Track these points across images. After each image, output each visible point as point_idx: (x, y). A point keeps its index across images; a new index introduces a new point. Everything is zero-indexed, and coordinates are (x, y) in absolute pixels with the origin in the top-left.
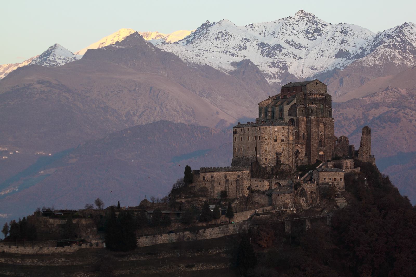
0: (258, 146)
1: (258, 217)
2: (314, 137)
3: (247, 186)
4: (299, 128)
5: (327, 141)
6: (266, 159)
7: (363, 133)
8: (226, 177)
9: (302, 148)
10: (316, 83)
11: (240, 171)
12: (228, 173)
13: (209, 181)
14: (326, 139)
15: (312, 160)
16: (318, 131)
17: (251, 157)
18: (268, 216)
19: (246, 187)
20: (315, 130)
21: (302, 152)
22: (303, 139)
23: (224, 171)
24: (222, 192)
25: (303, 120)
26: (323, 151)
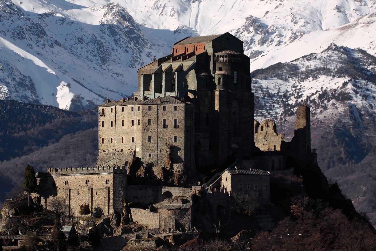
1: (138, 244)
4: (201, 108)
6: (150, 156)
7: (299, 115)
8: (87, 182)
10: (226, 38)
11: (110, 173)
12: (91, 176)
13: (62, 189)
17: (127, 152)
18: (153, 243)
23: (85, 174)
24: (82, 206)
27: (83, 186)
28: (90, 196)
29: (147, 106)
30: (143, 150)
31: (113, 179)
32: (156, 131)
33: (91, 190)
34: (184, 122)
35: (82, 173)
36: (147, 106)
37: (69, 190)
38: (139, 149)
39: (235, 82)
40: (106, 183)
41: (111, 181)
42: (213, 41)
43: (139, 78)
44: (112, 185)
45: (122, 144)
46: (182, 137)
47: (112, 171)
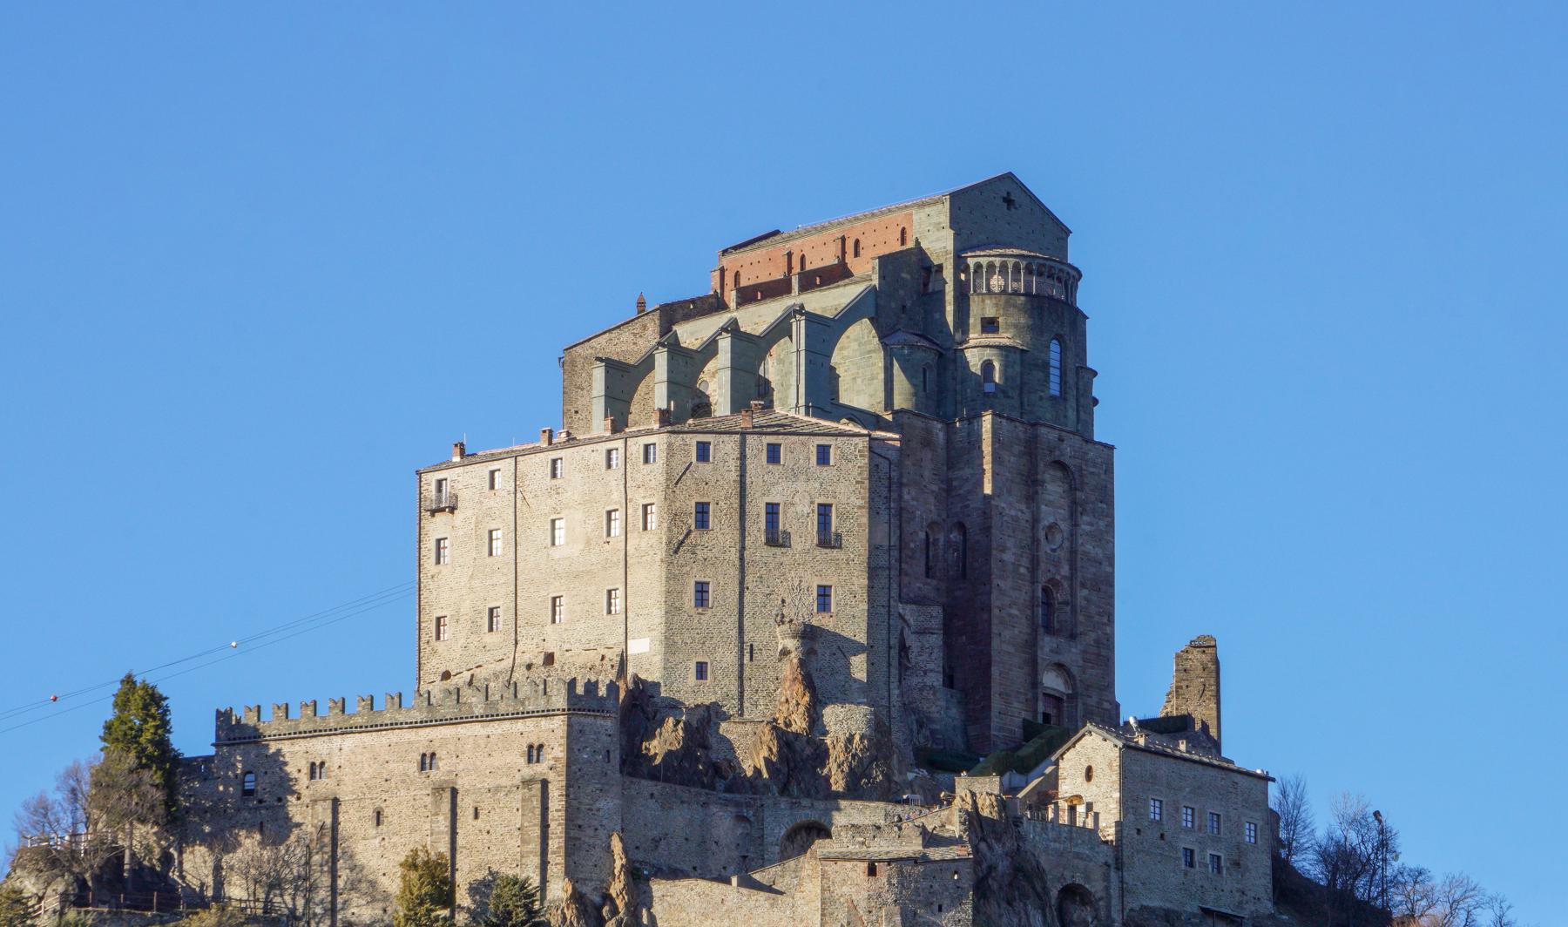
0: (637, 576)
2: (1008, 557)
3: (596, 823)
4: (905, 490)
5: (1084, 603)
6: (701, 670)
7: (1183, 684)
9: (922, 632)
11: (547, 714)
14: (1083, 586)
15: (995, 721)
16: (1035, 521)
19: (590, 832)
20: (1013, 513)
21: (929, 654)
22: (929, 572)
25: (927, 442)
26: (1060, 666)
27: (403, 781)
28: (443, 823)
29: (692, 440)
30: (670, 645)
31: (564, 741)
32: (734, 555)
33: (447, 795)
34: (865, 520)
35: (401, 718)
36: (692, 440)
37: (328, 804)
38: (647, 640)
39: (1054, 389)
40: (530, 761)
41: (557, 751)
42: (953, 196)
43: (571, 389)
44: (562, 767)
45: (549, 628)
46: (855, 588)
47: (560, 700)
